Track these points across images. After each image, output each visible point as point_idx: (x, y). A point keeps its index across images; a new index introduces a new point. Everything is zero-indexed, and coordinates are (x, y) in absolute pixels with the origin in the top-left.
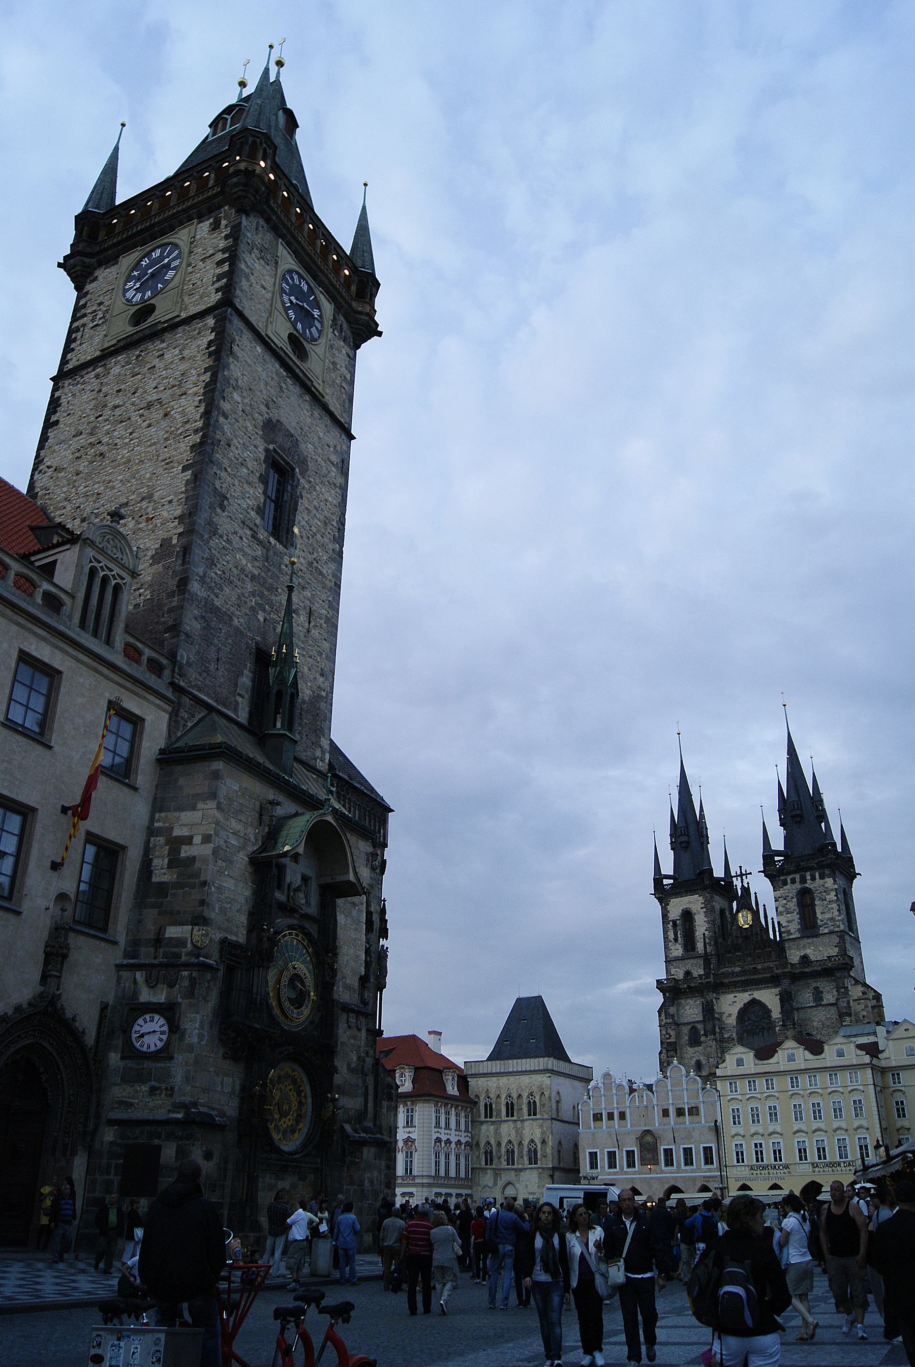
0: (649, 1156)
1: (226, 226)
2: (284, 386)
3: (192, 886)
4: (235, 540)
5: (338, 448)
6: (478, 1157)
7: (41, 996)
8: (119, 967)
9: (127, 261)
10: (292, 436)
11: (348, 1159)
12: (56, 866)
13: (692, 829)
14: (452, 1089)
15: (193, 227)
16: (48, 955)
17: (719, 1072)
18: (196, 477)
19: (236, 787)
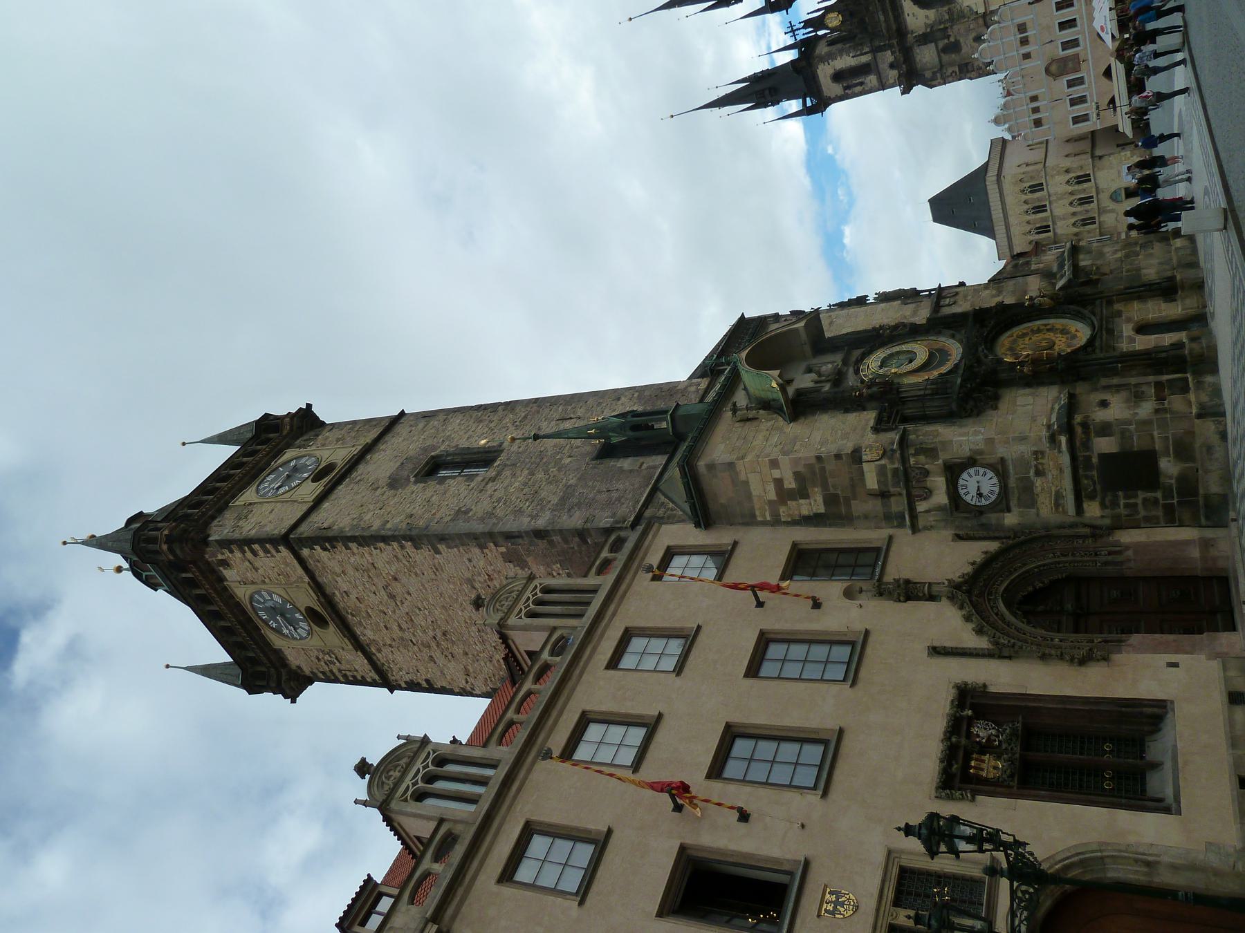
0: (1070, 65)
3: (823, 469)
4: (498, 494)
6: (1089, 232)
7: (952, 598)
8: (915, 529)
11: (1095, 277)
12: (817, 605)
13: (758, 87)
16: (908, 599)
17: (981, 10)
18: (443, 538)
19: (722, 447)
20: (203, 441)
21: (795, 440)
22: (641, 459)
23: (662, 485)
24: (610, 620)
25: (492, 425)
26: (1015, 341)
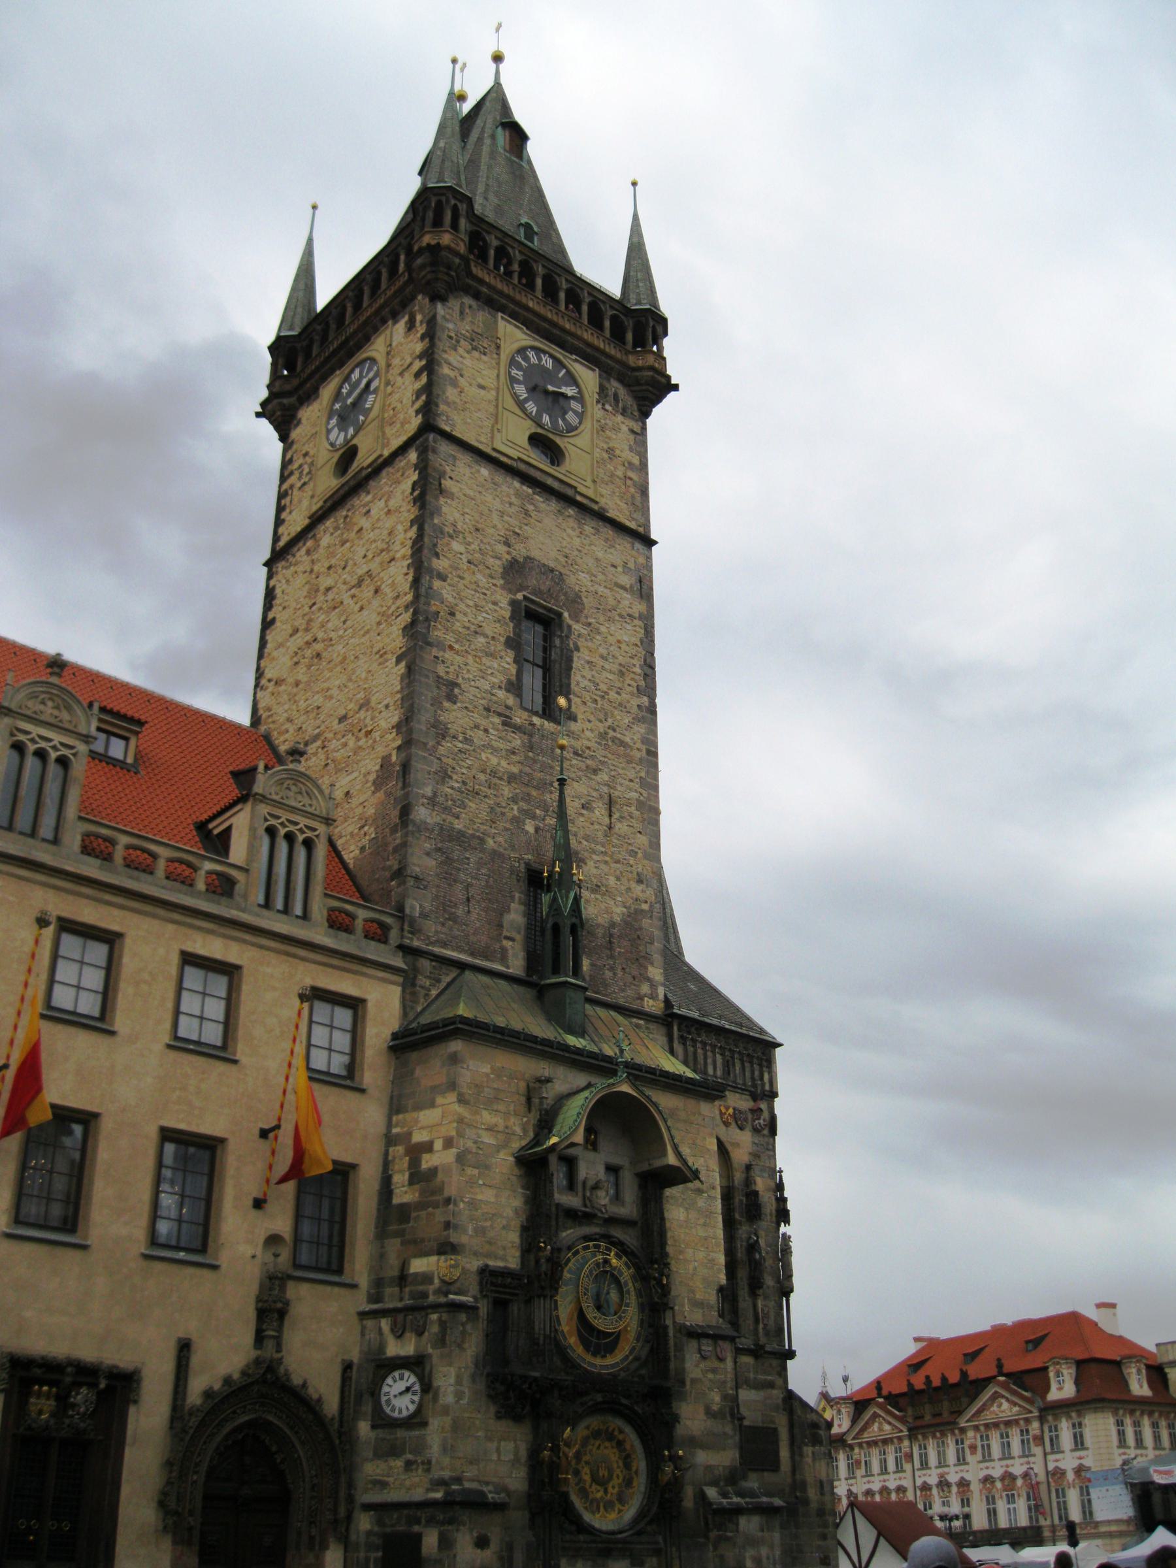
1: (421, 322)
2: (531, 508)
3: (436, 1206)
4: (478, 737)
5: (631, 565)
7: (257, 1362)
8: (363, 1315)
9: (327, 392)
10: (552, 571)
11: (713, 1534)
12: (258, 1204)
14: (1139, 1387)
15: (388, 332)
16: (262, 1314)
18: (410, 669)
19: (486, 1069)
20: (636, 218)
21: (484, 1167)
22: (519, 937)
23: (468, 974)
24: (253, 944)
25: (612, 695)
26: (610, 1437)
